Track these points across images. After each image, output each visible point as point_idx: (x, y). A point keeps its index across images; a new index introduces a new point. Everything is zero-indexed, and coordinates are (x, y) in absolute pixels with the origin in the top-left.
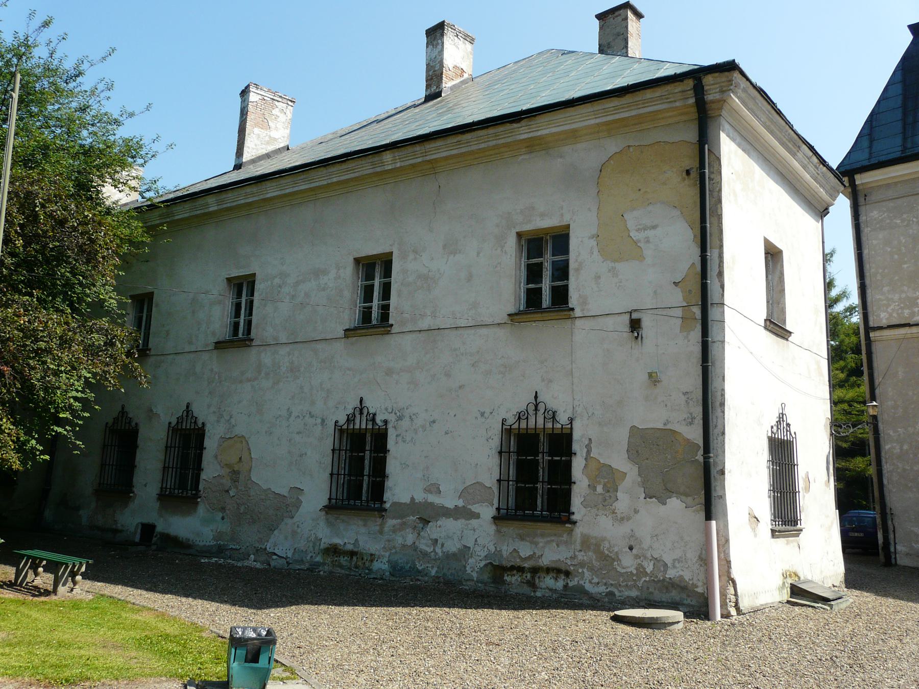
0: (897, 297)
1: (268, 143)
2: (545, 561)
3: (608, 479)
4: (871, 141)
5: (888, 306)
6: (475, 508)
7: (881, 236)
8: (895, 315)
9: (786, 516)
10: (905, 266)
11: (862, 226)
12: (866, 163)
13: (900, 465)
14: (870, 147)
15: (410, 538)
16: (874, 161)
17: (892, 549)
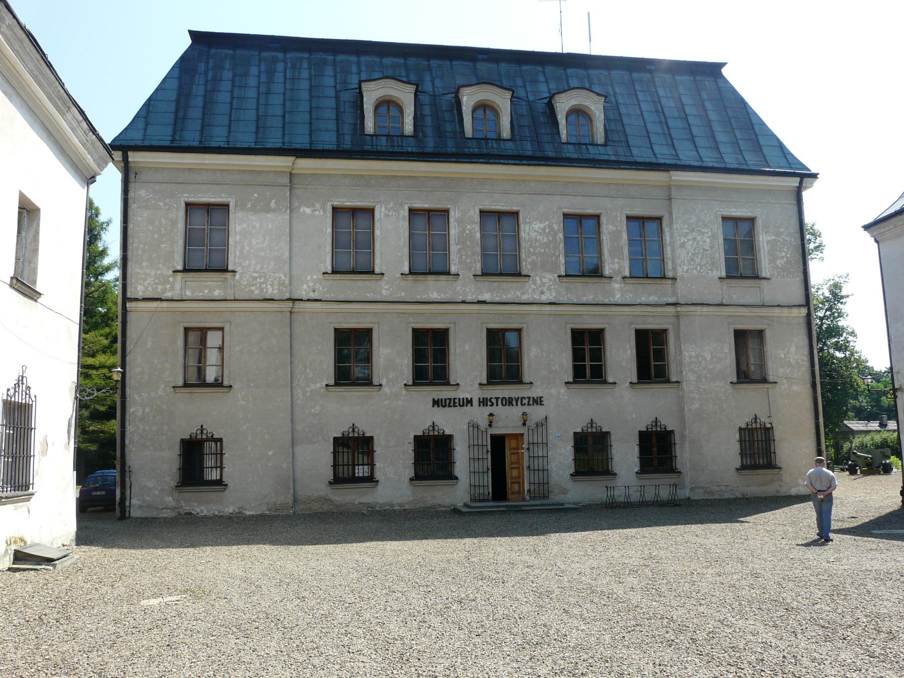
0: (153, 273)
4: (147, 124)
5: (145, 280)
7: (145, 214)
8: (150, 289)
10: (163, 246)
11: (130, 201)
12: (140, 143)
13: (141, 426)
14: (145, 130)
16: (147, 143)
17: (127, 504)
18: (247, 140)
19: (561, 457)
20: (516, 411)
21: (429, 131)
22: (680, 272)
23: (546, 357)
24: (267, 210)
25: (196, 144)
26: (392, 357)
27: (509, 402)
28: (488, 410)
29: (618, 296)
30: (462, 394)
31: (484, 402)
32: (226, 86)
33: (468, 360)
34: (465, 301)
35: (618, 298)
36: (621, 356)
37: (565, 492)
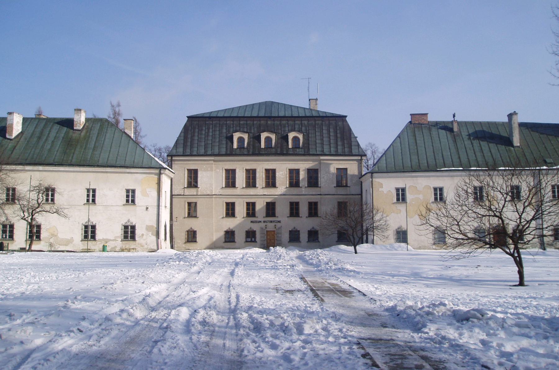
20: (273, 224)
22: (322, 185)
23: (282, 210)
25: (189, 154)
27: (271, 222)
28: (266, 224)
30: (259, 220)
31: (264, 222)
32: (196, 134)
35: (303, 193)
36: (304, 209)
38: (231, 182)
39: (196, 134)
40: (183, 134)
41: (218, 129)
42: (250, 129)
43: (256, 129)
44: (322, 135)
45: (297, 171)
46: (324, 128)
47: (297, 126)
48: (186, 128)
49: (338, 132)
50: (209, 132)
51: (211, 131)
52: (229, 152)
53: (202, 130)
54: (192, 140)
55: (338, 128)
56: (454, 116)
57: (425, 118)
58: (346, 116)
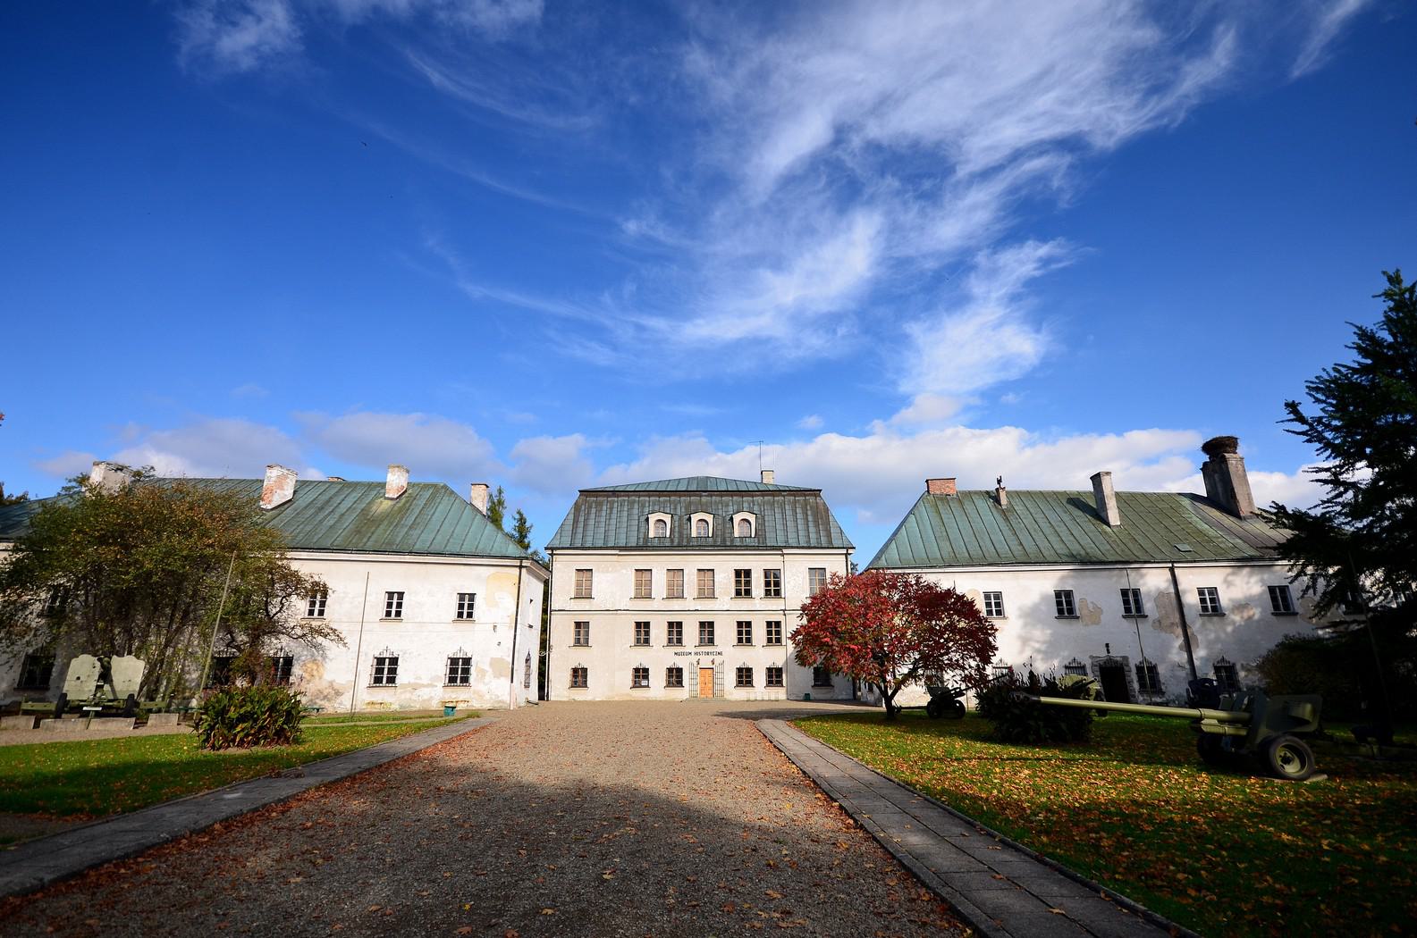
1: (283, 498)
2: (460, 699)
3: (483, 673)
6: (436, 684)
9: (527, 686)
15: (408, 695)
18: (600, 543)
19: (731, 678)
20: (711, 657)
21: (676, 535)
23: (726, 633)
24: (608, 572)
25: (579, 545)
26: (659, 633)
28: (699, 657)
29: (758, 605)
30: (687, 650)
31: (696, 654)
32: (593, 516)
33: (691, 633)
34: (691, 611)
36: (759, 633)
37: (731, 694)
38: (643, 592)
39: (593, 516)
40: (572, 517)
41: (626, 509)
42: (675, 509)
43: (683, 510)
44: (784, 518)
45: (748, 573)
46: (787, 507)
47: (746, 505)
48: (577, 507)
49: (809, 513)
50: (611, 513)
51: (615, 511)
52: (641, 544)
53: (601, 510)
54: (585, 525)
55: (808, 508)
56: (999, 482)
57: (951, 485)
58: (820, 491)
